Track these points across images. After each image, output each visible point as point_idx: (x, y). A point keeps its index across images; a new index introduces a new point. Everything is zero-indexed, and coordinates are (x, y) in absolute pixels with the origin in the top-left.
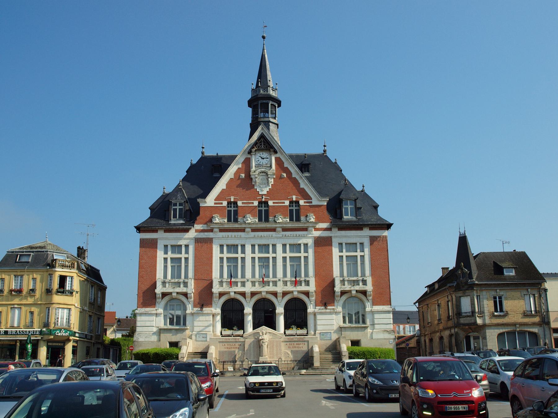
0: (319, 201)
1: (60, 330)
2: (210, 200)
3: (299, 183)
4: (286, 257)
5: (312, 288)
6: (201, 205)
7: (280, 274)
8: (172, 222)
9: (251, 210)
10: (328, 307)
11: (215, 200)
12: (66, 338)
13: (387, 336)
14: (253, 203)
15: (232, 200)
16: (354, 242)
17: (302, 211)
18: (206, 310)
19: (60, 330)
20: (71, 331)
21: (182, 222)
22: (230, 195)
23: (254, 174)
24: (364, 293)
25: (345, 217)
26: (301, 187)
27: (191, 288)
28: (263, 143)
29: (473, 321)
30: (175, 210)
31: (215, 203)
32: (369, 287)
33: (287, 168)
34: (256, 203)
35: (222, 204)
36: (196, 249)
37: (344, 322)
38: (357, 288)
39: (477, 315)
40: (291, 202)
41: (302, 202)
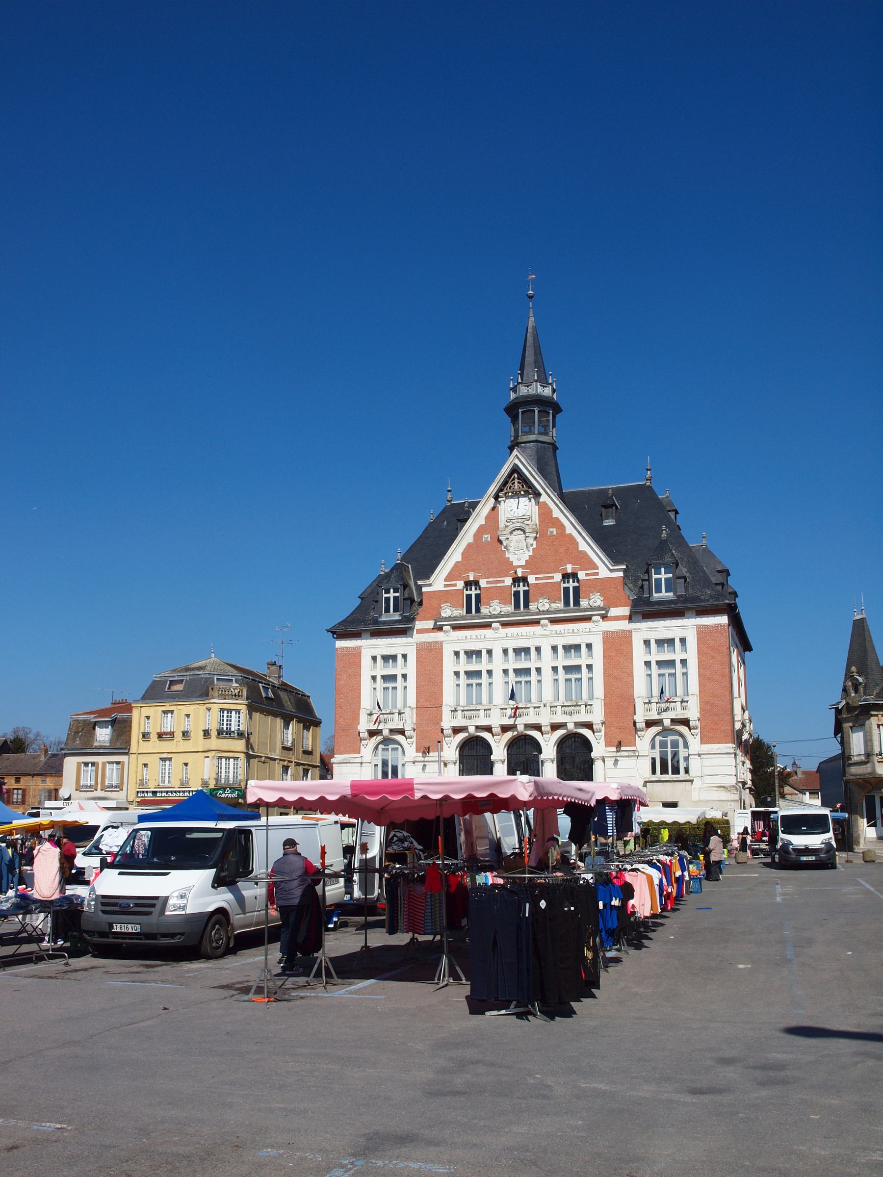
0: (611, 571)
1: (224, 789)
2: (437, 582)
3: (577, 543)
4: (557, 667)
5: (597, 716)
6: (424, 589)
7: (548, 695)
8: (384, 618)
9: (499, 593)
10: (623, 748)
11: (445, 580)
12: (235, 801)
13: (723, 795)
14: (503, 581)
15: (471, 578)
16: (670, 636)
17: (582, 590)
18: (433, 755)
19: (224, 789)
20: (240, 791)
21: (397, 617)
22: (467, 571)
23: (504, 533)
24: (686, 722)
25: (655, 595)
26: (580, 549)
27: (409, 721)
28: (516, 481)
29: (869, 770)
30: (387, 599)
31: (445, 586)
32: (693, 713)
33: (557, 519)
34: (508, 581)
35: (455, 585)
36: (418, 661)
37: (654, 772)
38: (672, 715)
39: (876, 759)
40: (566, 576)
41: (581, 575)
